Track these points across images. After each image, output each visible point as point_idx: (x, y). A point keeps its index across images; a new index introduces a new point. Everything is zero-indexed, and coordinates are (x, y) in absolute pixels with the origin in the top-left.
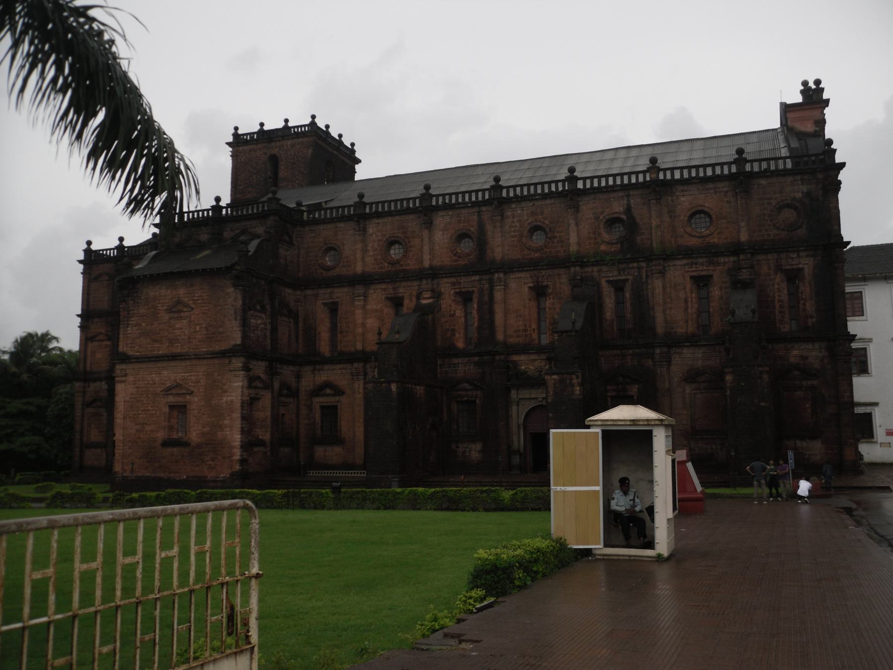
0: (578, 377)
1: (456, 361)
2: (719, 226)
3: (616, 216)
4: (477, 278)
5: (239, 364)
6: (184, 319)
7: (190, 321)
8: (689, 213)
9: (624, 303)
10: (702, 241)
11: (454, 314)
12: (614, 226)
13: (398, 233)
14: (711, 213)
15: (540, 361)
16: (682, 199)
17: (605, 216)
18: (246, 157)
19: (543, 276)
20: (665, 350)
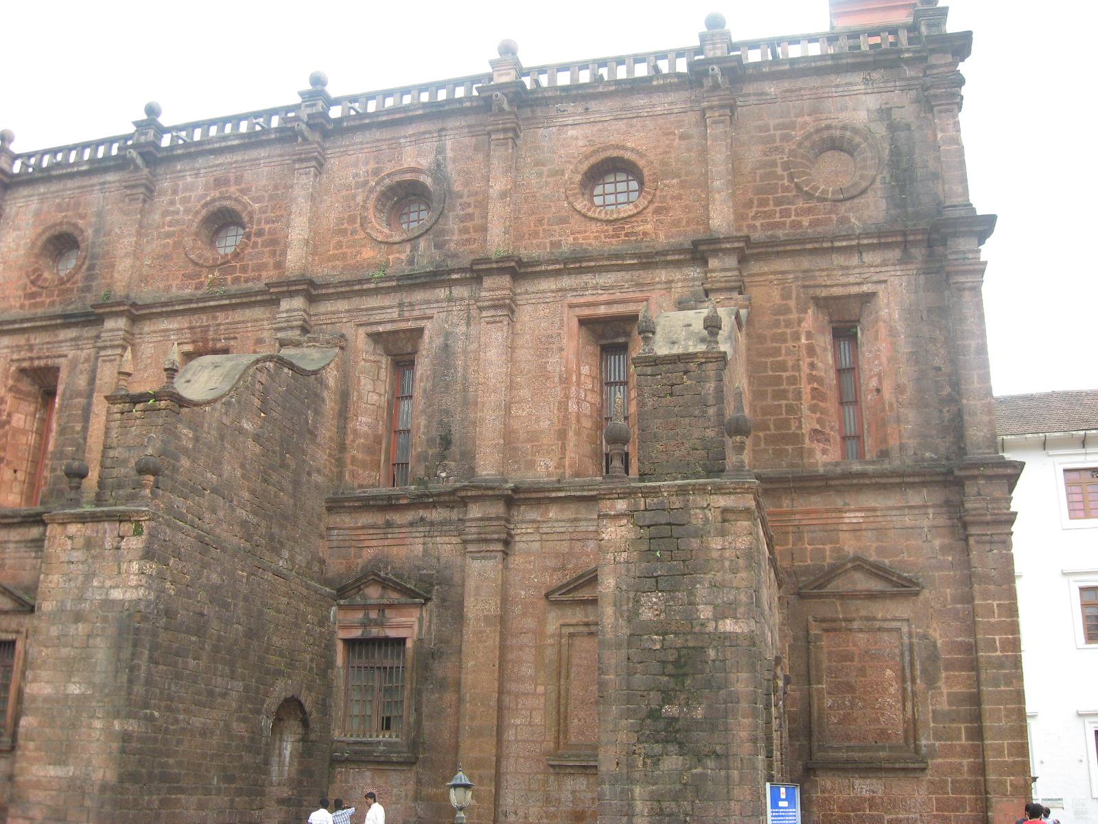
2: (658, 193)
3: (408, 177)
4: (72, 333)
8: (585, 166)
10: (614, 230)
11: (8, 422)
12: (406, 210)
14: (641, 163)
16: (571, 132)
17: (383, 179)
19: (219, 325)
20: (498, 509)
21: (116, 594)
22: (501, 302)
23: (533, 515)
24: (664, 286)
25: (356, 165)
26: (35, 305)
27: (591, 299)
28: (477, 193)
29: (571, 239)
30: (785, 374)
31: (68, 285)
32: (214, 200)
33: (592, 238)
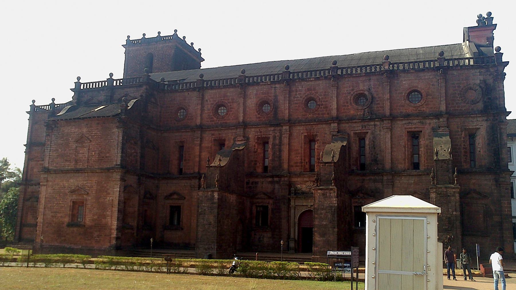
0: (334, 192)
1: (256, 180)
3: (361, 92)
4: (272, 128)
5: (118, 177)
6: (85, 148)
7: (89, 149)
8: (408, 92)
9: (364, 147)
11: (257, 151)
13: (224, 99)
14: (422, 92)
15: (310, 182)
16: (404, 82)
17: (355, 92)
18: (134, 54)
23: (398, 178)
27: (410, 127)
28: (380, 98)
29: (405, 111)
30: (458, 147)
31: (269, 116)
33: (410, 110)
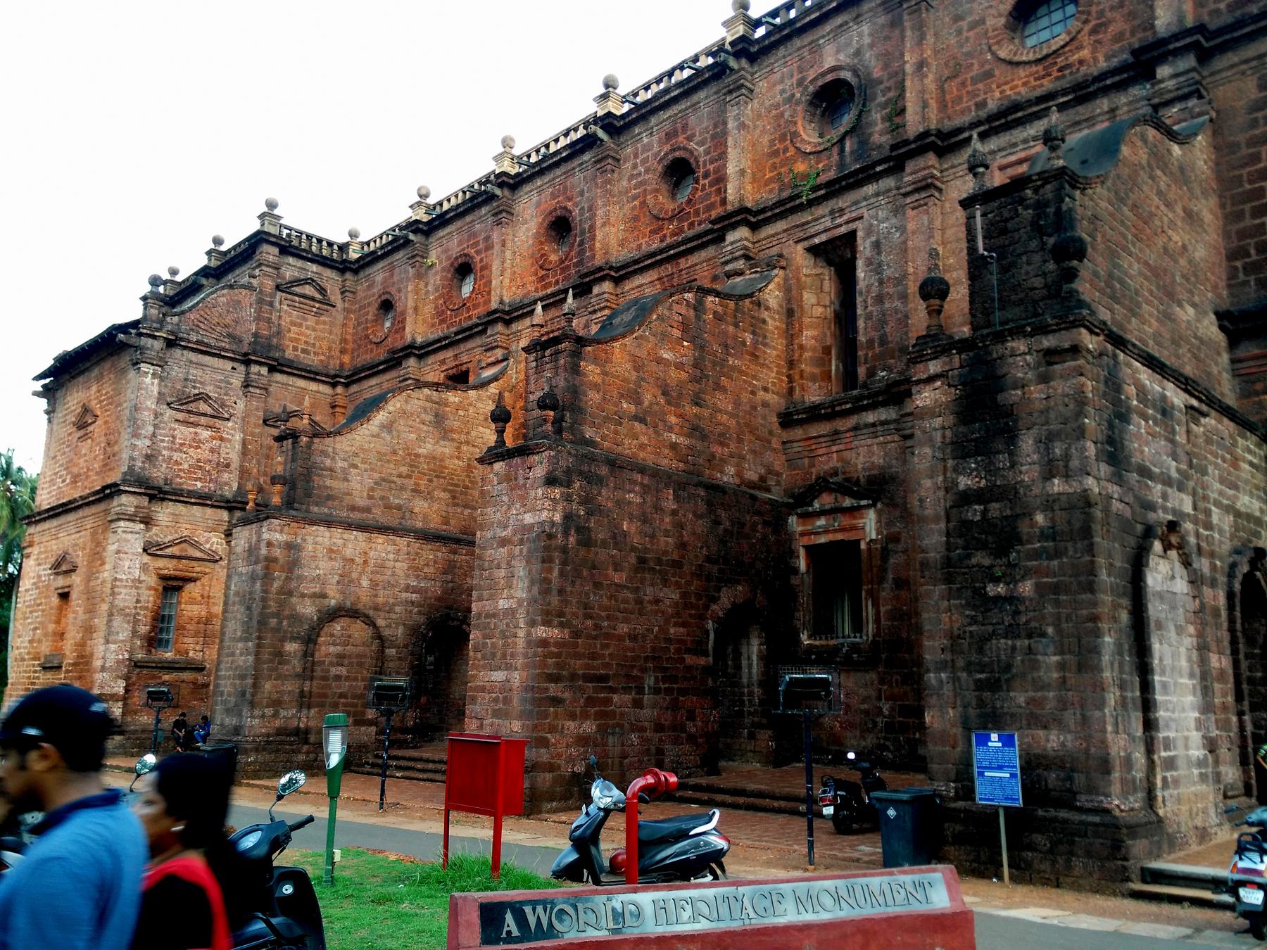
3: (829, 78)
10: (1045, 68)
21: (529, 519)
22: (924, 183)
24: (1107, 116)
25: (782, 81)
26: (545, 287)
27: (1022, 155)
29: (997, 95)
32: (667, 154)
33: (1020, 86)
